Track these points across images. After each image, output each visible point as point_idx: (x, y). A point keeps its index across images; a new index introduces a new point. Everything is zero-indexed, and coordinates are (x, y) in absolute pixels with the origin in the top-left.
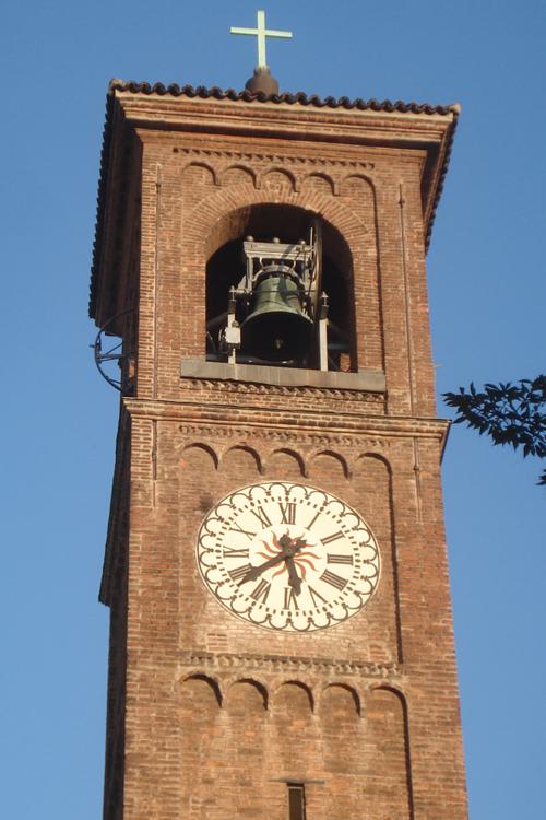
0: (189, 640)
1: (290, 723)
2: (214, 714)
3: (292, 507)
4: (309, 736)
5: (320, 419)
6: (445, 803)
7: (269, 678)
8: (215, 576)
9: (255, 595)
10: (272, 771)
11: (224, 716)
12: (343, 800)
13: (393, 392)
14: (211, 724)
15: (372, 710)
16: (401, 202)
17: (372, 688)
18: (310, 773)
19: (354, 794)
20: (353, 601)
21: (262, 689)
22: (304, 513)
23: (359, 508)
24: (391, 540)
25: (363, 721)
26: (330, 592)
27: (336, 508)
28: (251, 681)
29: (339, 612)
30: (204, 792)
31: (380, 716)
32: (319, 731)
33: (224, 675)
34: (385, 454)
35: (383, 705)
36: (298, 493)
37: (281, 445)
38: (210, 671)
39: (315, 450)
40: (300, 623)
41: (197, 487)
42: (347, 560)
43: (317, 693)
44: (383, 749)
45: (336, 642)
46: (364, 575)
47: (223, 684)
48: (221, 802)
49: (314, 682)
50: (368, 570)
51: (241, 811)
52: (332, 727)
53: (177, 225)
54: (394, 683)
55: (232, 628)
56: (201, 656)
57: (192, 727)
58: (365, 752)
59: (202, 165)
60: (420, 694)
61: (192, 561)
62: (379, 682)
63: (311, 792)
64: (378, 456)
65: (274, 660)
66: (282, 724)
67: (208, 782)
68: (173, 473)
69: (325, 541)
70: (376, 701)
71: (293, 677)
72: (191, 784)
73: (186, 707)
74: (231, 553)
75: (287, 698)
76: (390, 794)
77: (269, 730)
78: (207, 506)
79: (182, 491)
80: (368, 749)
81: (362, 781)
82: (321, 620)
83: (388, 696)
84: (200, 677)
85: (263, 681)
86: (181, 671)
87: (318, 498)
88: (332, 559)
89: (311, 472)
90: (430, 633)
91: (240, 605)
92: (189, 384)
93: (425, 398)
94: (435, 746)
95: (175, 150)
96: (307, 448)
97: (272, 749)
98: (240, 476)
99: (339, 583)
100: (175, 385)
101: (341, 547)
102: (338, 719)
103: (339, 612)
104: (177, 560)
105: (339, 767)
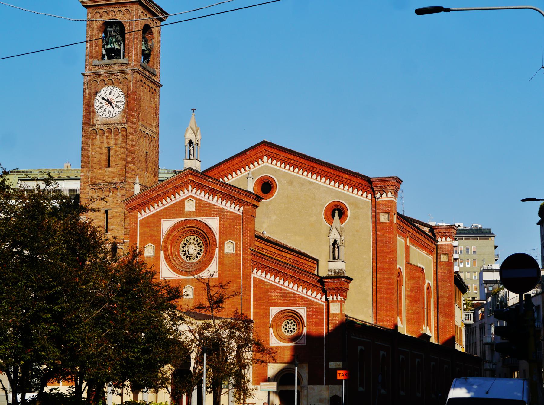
0: (93, 122)
1: (108, 136)
2: (96, 136)
4: (111, 138)
5: (115, 72)
6: (131, 149)
7: (105, 129)
8: (97, 108)
9: (104, 112)
10: (105, 145)
11: (98, 136)
12: (116, 150)
13: (130, 63)
14: (96, 138)
15: (122, 132)
16: (134, 15)
17: (122, 128)
18: (111, 145)
19: (118, 149)
20: (120, 110)
21: (104, 130)
22: (113, 92)
23: (122, 90)
24: (127, 95)
25: (120, 134)
27: (118, 90)
29: (117, 113)
30: (94, 151)
31: (123, 133)
32: (113, 137)
33: (97, 129)
34: (127, 77)
35: (124, 131)
36: (112, 88)
37: (109, 78)
38: (95, 129)
39: (115, 79)
40: (111, 116)
41: (95, 89)
42: (119, 102)
43: (113, 130)
44: (123, 139)
46: (122, 105)
47: (97, 130)
48: (97, 153)
49: (112, 128)
50: (123, 103)
51: (100, 154)
52: (115, 136)
53: (93, 28)
54: (125, 126)
55: (100, 119)
56: (94, 125)
57: (93, 139)
58: (120, 140)
59: (98, 12)
61: (93, 106)
62: (122, 127)
63: (112, 148)
64: (126, 78)
66: (107, 136)
67: (95, 149)
68: (90, 88)
69: (116, 98)
70: (123, 130)
71: (108, 128)
72: (92, 150)
73: (92, 135)
75: (108, 131)
76: (123, 148)
77: (105, 138)
78: (97, 93)
79: (92, 91)
80: (121, 139)
81: (119, 146)
82: (114, 115)
83: (124, 129)
84: (94, 129)
85: (104, 129)
86: (91, 129)
87: (115, 89)
88: (117, 102)
89: (115, 83)
90: (132, 115)
91: (101, 114)
92: (94, 67)
93: (135, 63)
95: (93, 10)
96: (113, 78)
97: (105, 142)
98: (102, 86)
100: (92, 68)
101: (119, 99)
102: (116, 134)
103: (117, 113)
104: (91, 106)
105: (116, 144)
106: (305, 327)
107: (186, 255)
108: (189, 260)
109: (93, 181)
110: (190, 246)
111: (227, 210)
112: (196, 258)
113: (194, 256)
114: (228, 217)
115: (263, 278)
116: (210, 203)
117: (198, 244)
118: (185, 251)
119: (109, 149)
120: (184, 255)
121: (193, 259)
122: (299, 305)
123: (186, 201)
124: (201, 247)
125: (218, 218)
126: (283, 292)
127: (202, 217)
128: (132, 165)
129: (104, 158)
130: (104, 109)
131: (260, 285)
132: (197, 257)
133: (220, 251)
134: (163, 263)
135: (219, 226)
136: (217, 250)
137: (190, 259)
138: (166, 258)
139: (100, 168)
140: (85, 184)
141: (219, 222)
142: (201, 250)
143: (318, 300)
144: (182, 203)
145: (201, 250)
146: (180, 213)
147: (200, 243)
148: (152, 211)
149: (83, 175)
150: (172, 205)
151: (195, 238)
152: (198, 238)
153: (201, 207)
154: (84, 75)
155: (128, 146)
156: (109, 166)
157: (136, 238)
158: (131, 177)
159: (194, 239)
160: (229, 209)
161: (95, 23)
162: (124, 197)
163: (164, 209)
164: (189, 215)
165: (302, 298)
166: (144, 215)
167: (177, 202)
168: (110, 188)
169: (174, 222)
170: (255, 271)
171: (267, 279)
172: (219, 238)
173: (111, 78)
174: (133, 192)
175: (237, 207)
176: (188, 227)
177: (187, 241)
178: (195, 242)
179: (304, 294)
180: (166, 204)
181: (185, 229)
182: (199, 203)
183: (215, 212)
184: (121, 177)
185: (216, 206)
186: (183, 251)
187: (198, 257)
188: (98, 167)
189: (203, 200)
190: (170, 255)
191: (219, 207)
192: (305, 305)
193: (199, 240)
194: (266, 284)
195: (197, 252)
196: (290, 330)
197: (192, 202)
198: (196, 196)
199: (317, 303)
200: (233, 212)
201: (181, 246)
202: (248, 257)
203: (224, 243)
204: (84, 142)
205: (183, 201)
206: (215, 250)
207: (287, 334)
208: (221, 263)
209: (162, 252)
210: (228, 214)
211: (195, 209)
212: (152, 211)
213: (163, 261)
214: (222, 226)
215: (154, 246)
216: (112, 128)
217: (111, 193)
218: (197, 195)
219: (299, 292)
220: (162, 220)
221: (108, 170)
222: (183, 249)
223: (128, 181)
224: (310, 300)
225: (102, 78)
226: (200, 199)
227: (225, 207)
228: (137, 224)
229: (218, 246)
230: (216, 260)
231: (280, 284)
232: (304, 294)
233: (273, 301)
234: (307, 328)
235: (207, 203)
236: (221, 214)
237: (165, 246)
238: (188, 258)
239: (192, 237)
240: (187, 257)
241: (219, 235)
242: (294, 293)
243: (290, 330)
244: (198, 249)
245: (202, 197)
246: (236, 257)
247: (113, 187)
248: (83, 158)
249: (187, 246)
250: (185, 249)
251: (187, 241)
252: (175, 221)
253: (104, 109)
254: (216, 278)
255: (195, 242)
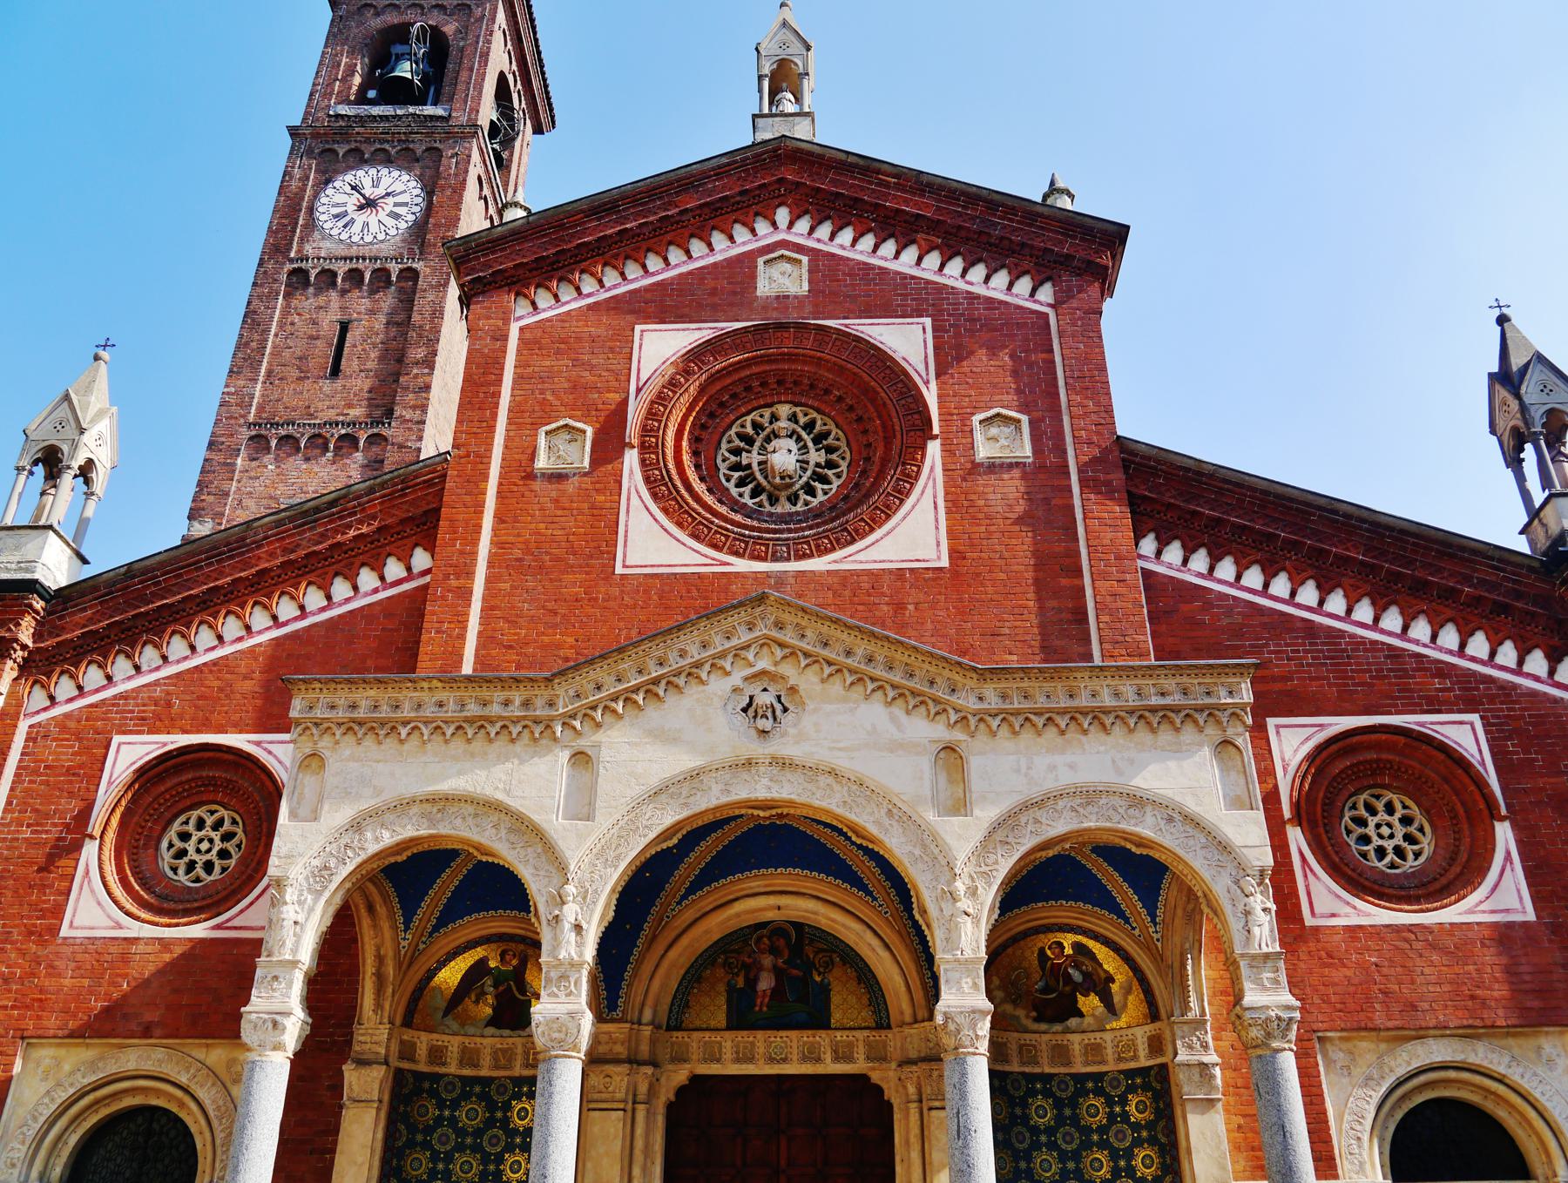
3: (379, 179)
8: (323, 218)
9: (345, 226)
20: (403, 225)
23: (421, 178)
26: (390, 222)
28: (329, 270)
29: (393, 232)
35: (407, 279)
40: (368, 239)
42: (406, 204)
45: (386, 250)
49: (366, 268)
54: (414, 265)
60: (428, 270)
65: (345, 259)
67: (292, 324)
72: (281, 326)
74: (337, 205)
82: (381, 237)
86: (289, 267)
91: (335, 232)
94: (431, 296)
96: (394, 147)
99: (396, 216)
103: (393, 232)
106: (1495, 815)
107: (750, 486)
108: (766, 504)
109: (264, 415)
110: (775, 443)
111: (968, 292)
112: (803, 496)
113: (798, 486)
114: (980, 320)
115: (1200, 575)
116: (880, 268)
117: (816, 441)
118: (749, 466)
119: (344, 328)
120: (741, 483)
121: (793, 499)
122: (1434, 705)
123: (760, 261)
124: (830, 450)
125: (928, 321)
126: (1323, 644)
127: (845, 318)
128: (426, 371)
129: (323, 352)
130: (347, 219)
131: (1185, 608)
132: (811, 491)
133: (947, 451)
134: (635, 501)
135: (936, 355)
136: (934, 449)
137: (773, 500)
138: (647, 480)
139: (299, 379)
140: (233, 421)
141: (934, 337)
142: (830, 465)
143: (1537, 679)
144: (743, 267)
145: (830, 465)
146: (732, 305)
147: (826, 435)
148: (589, 295)
149: (233, 394)
150: (690, 273)
151: (800, 415)
152: (815, 415)
153: (838, 280)
154: (293, 132)
155: (416, 317)
156: (336, 371)
157: (497, 395)
158: (414, 408)
159: (793, 418)
160: (980, 290)
161: (357, 27)
162: (377, 465)
163: (648, 289)
164: (776, 309)
165: (1443, 670)
166: (544, 310)
167: (715, 265)
168: (328, 435)
169: (697, 335)
170: (1148, 545)
171: (1220, 581)
172: (941, 397)
173: (387, 146)
174: (419, 450)
175: (1024, 285)
176: (768, 359)
177: (756, 426)
178: (799, 430)
179: (1450, 652)
180: (663, 270)
181: (755, 369)
182: (824, 267)
183: (912, 300)
184: (377, 406)
185: (913, 277)
186: (736, 467)
187: (820, 492)
188: (297, 374)
189: (848, 259)
190: (671, 465)
191: (928, 282)
192: (1469, 704)
193: (819, 422)
194: (1219, 607)
195: (809, 473)
196: (1389, 845)
197: (787, 267)
198: (811, 244)
199: (1534, 694)
200: (1001, 302)
201: (724, 446)
202: (1110, 477)
203: (965, 419)
204: (255, 302)
205: (750, 257)
206: (923, 448)
207: (1427, 844)
208: (959, 505)
209: (631, 458)
210: (978, 309)
211: (806, 287)
212: (589, 295)
213: (633, 491)
214: (947, 356)
215: (590, 431)
216: (366, 268)
217: (329, 455)
218: (819, 240)
219: (1417, 642)
220: (638, 328)
221: (327, 386)
222: (733, 459)
223: (401, 416)
224: (1490, 680)
225: (353, 145)
226: (833, 255)
227: (960, 285)
228: (505, 338)
229: (936, 430)
230: (929, 491)
231: (1299, 606)
232: (1450, 652)
233: (1278, 686)
234: (1514, 826)
235: (867, 267)
236: (944, 310)
237: (646, 431)
238: (764, 497)
239: (784, 410)
240: (754, 494)
241: (939, 389)
242: (1390, 647)
243: (1389, 845)
244: (816, 457)
245: (842, 247)
246: (1041, 476)
247: (343, 432)
248: (241, 345)
249: (757, 444)
250: (753, 458)
251: (756, 426)
252: (705, 332)
253: (347, 219)
254: (940, 569)
255: (799, 430)
